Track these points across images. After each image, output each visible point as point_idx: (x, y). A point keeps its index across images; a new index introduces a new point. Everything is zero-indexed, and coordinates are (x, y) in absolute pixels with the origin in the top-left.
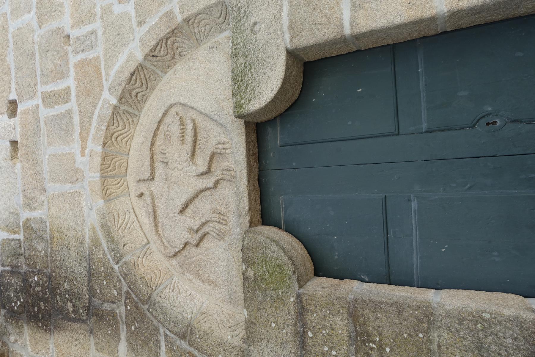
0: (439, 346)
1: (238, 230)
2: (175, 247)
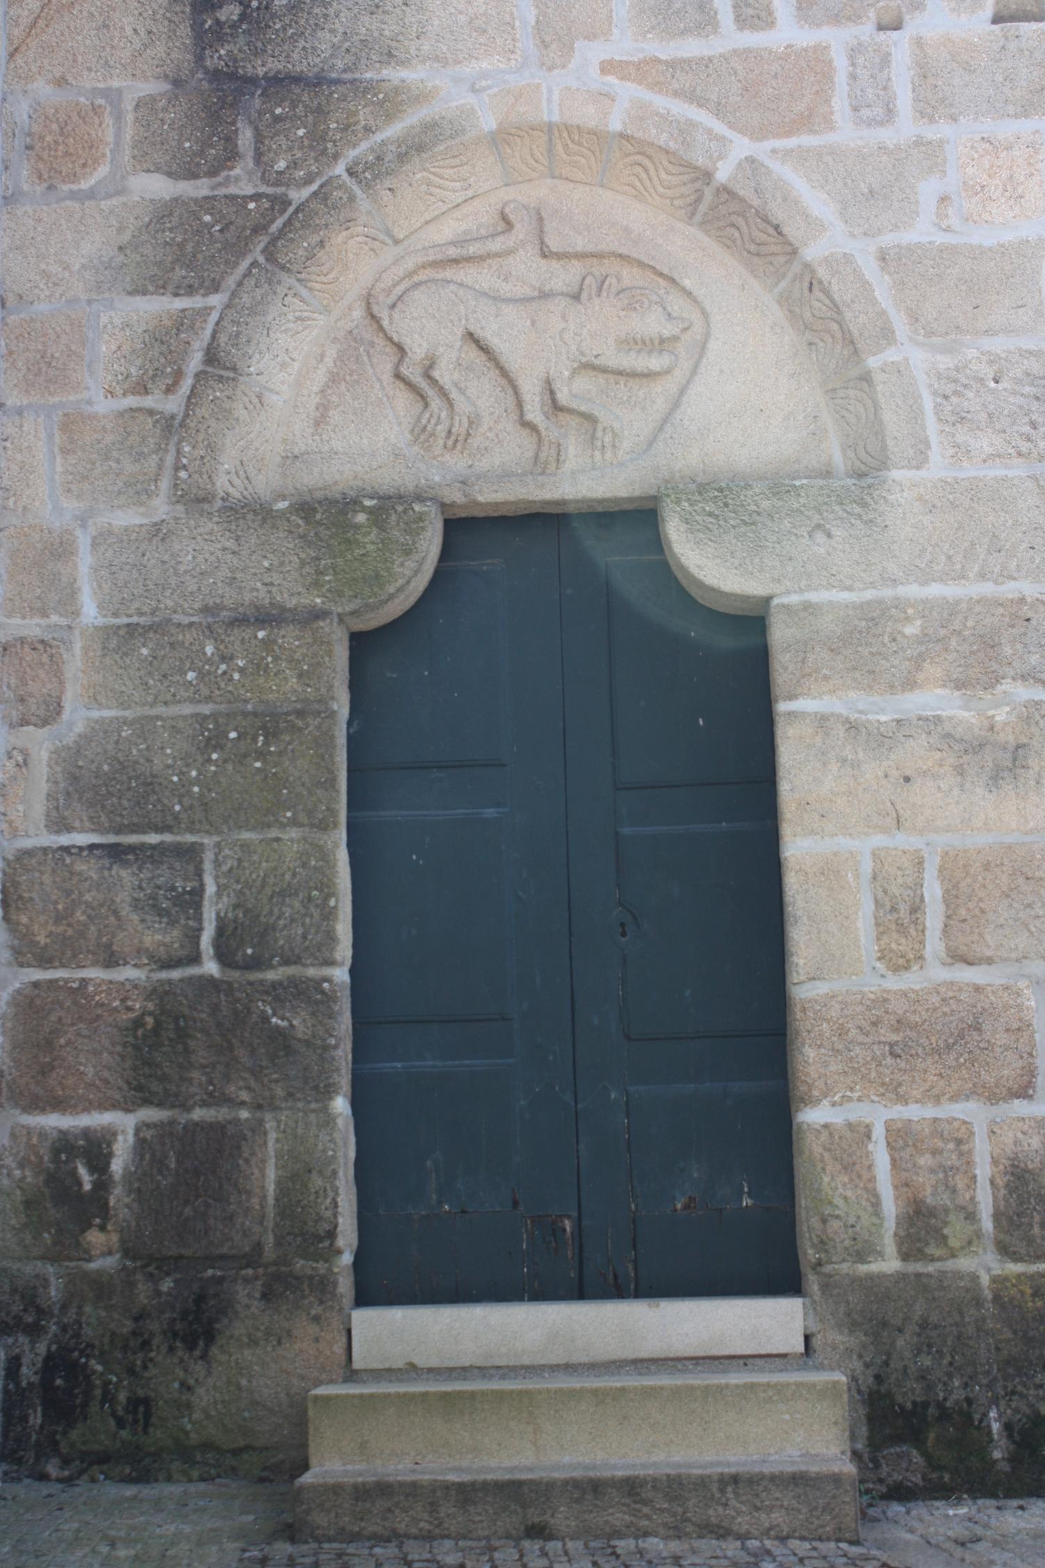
0: (277, 840)
1: (437, 479)
2: (391, 316)
